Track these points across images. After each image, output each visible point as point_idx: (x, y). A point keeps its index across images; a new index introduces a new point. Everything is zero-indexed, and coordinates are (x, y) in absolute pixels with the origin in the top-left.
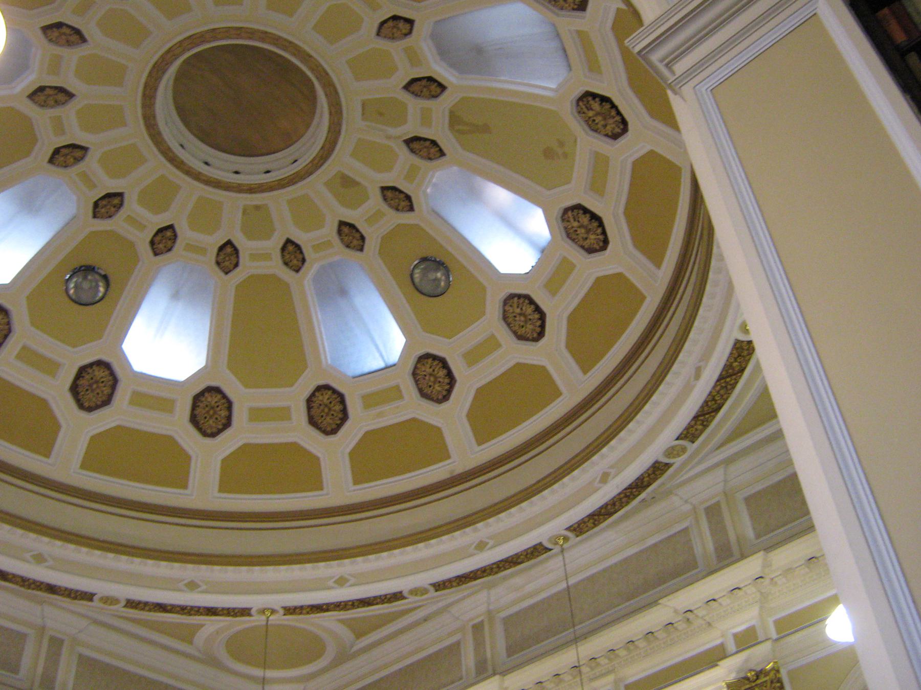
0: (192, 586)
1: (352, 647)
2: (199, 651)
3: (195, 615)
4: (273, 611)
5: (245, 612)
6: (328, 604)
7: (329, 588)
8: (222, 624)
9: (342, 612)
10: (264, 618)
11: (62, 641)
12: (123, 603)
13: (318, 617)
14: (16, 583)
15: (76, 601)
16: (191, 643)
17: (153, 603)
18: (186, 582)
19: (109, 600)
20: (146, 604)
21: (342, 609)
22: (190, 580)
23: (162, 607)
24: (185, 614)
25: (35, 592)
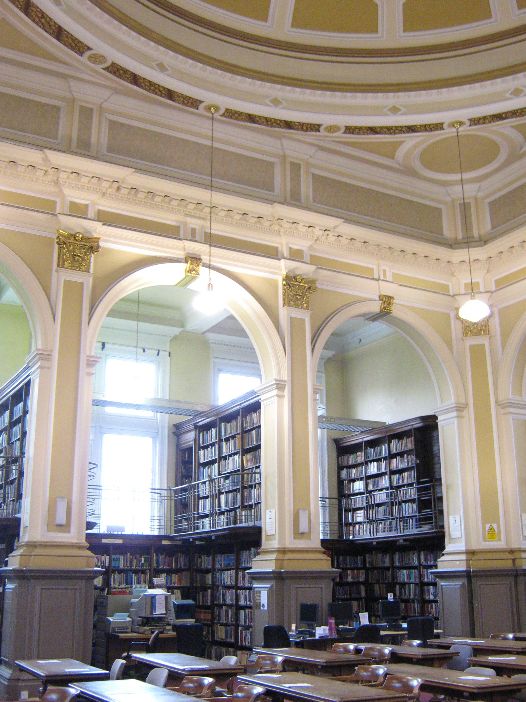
0: (394, 110)
1: (521, 149)
2: (399, 164)
3: (399, 133)
4: (461, 123)
5: (439, 127)
6: (506, 113)
7: (507, 99)
8: (420, 139)
9: (518, 119)
10: (454, 130)
11: (299, 165)
12: (343, 130)
13: (495, 126)
14: (262, 124)
15: (308, 133)
16: (393, 159)
17: (366, 128)
18: (388, 108)
19: (332, 129)
20: (361, 128)
21: (519, 116)
22: (391, 106)
23: (372, 130)
24: (391, 133)
25: (276, 129)
